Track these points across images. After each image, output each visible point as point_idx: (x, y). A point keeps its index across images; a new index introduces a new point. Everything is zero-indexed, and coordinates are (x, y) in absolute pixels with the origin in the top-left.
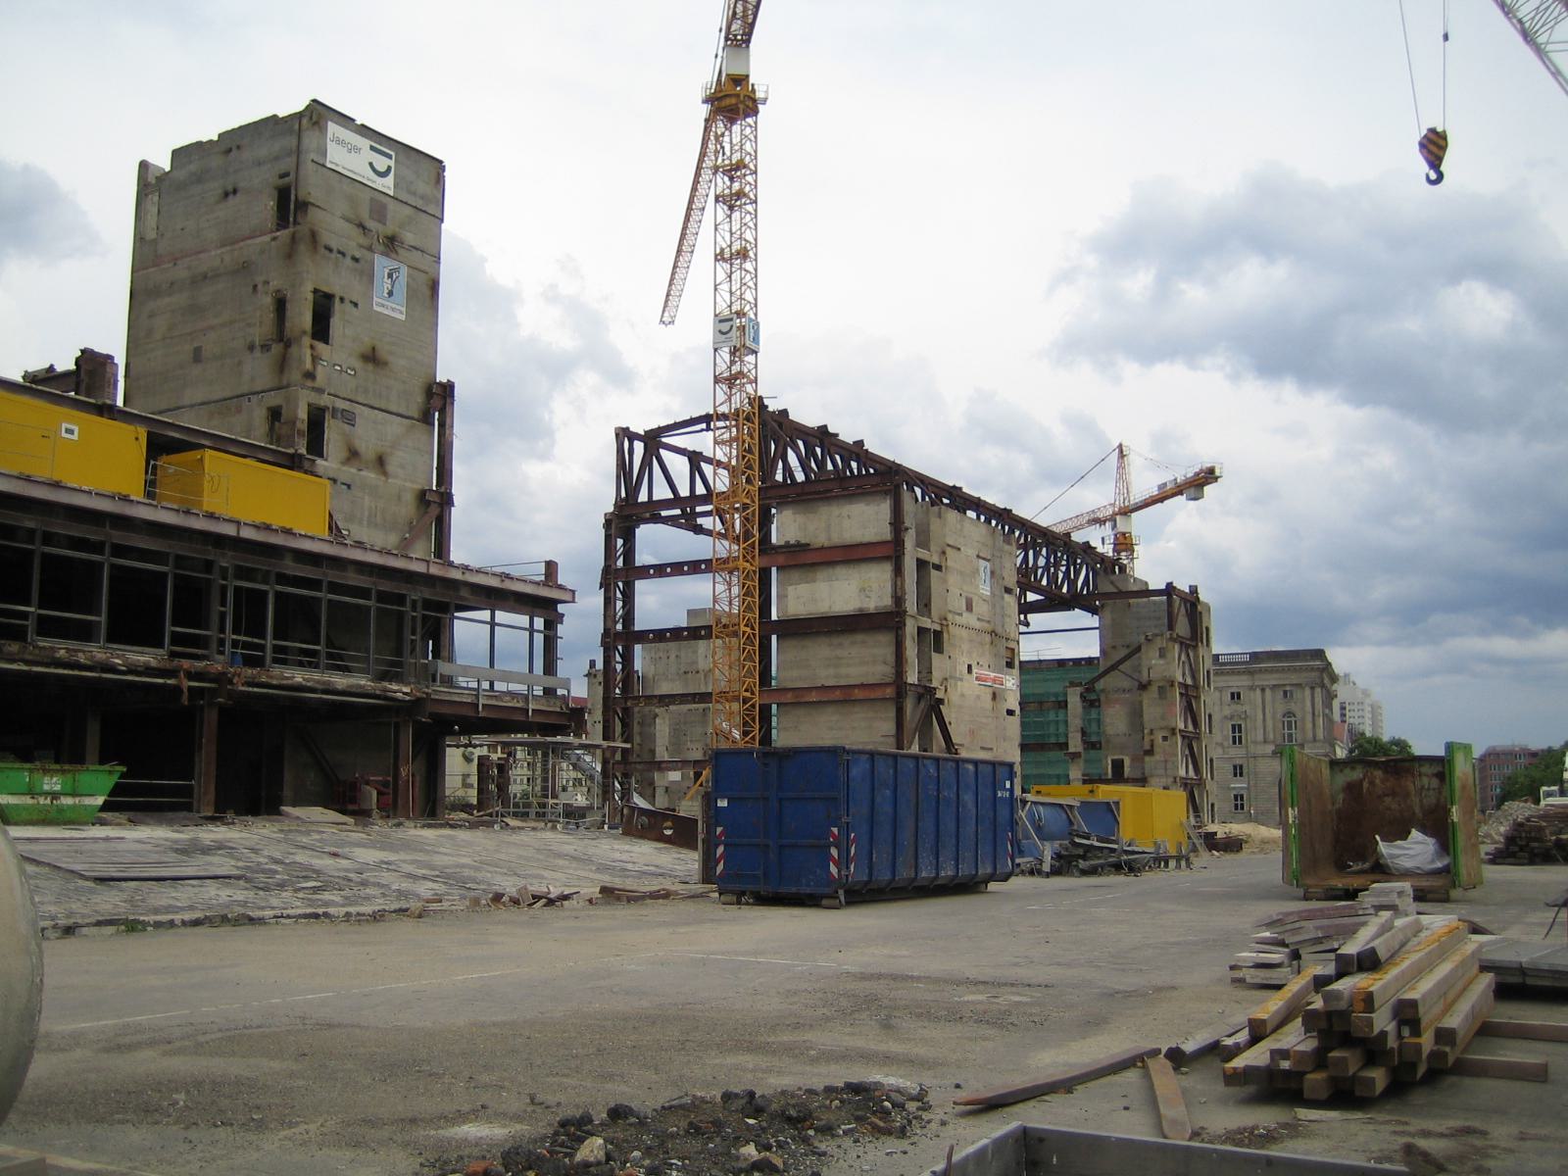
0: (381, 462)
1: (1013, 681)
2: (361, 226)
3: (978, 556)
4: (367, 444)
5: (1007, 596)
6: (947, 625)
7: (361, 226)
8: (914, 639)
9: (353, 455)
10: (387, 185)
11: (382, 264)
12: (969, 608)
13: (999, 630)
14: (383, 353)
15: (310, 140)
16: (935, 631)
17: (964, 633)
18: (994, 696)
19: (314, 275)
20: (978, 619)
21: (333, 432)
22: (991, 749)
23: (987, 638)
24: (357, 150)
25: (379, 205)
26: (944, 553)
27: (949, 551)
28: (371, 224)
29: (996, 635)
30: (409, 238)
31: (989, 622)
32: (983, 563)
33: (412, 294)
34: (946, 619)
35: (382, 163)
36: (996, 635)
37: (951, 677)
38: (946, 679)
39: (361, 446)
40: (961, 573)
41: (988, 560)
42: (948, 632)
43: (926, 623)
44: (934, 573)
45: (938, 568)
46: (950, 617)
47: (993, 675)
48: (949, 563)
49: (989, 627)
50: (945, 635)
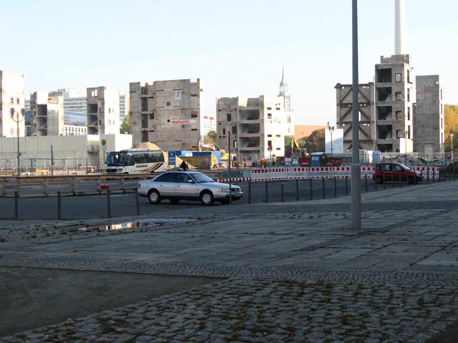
1: (196, 121)
3: (174, 90)
5: (192, 98)
6: (156, 111)
8: (139, 118)
12: (168, 104)
13: (187, 107)
16: (150, 114)
17: (165, 112)
18: (183, 126)
20: (174, 107)
22: (182, 141)
23: (181, 111)
26: (155, 93)
27: (157, 92)
29: (184, 109)
31: (181, 106)
32: (176, 92)
34: (155, 110)
36: (184, 109)
37: (158, 124)
38: (155, 125)
40: (163, 96)
41: (181, 90)
42: (157, 113)
43: (146, 113)
44: (149, 99)
45: (153, 98)
46: (157, 109)
47: (182, 121)
48: (157, 95)
49: (181, 108)
50: (155, 114)
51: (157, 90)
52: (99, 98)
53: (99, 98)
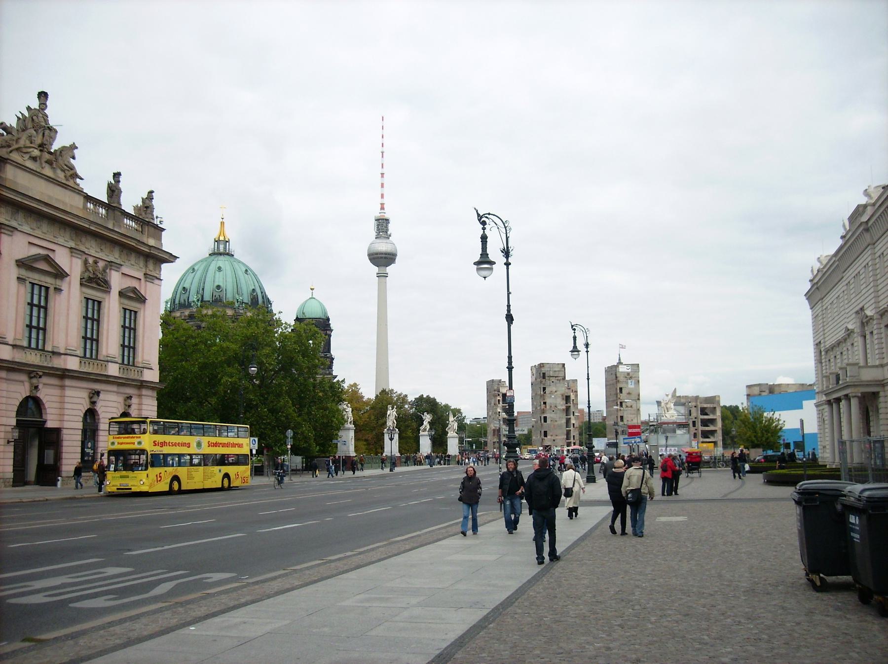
0: (631, 406)
2: (626, 377)
4: (629, 405)
7: (626, 377)
9: (627, 406)
10: (630, 370)
11: (629, 381)
14: (631, 392)
15: (617, 369)
19: (620, 386)
21: (624, 404)
24: (624, 368)
25: (628, 374)
28: (628, 376)
30: (634, 376)
33: (635, 383)
35: (628, 368)
39: (628, 405)
51: (782, 390)
52: (572, 390)
53: (572, 390)
